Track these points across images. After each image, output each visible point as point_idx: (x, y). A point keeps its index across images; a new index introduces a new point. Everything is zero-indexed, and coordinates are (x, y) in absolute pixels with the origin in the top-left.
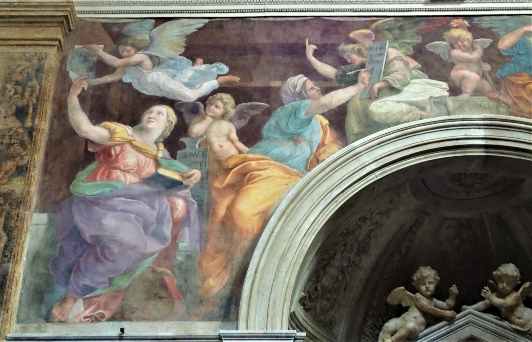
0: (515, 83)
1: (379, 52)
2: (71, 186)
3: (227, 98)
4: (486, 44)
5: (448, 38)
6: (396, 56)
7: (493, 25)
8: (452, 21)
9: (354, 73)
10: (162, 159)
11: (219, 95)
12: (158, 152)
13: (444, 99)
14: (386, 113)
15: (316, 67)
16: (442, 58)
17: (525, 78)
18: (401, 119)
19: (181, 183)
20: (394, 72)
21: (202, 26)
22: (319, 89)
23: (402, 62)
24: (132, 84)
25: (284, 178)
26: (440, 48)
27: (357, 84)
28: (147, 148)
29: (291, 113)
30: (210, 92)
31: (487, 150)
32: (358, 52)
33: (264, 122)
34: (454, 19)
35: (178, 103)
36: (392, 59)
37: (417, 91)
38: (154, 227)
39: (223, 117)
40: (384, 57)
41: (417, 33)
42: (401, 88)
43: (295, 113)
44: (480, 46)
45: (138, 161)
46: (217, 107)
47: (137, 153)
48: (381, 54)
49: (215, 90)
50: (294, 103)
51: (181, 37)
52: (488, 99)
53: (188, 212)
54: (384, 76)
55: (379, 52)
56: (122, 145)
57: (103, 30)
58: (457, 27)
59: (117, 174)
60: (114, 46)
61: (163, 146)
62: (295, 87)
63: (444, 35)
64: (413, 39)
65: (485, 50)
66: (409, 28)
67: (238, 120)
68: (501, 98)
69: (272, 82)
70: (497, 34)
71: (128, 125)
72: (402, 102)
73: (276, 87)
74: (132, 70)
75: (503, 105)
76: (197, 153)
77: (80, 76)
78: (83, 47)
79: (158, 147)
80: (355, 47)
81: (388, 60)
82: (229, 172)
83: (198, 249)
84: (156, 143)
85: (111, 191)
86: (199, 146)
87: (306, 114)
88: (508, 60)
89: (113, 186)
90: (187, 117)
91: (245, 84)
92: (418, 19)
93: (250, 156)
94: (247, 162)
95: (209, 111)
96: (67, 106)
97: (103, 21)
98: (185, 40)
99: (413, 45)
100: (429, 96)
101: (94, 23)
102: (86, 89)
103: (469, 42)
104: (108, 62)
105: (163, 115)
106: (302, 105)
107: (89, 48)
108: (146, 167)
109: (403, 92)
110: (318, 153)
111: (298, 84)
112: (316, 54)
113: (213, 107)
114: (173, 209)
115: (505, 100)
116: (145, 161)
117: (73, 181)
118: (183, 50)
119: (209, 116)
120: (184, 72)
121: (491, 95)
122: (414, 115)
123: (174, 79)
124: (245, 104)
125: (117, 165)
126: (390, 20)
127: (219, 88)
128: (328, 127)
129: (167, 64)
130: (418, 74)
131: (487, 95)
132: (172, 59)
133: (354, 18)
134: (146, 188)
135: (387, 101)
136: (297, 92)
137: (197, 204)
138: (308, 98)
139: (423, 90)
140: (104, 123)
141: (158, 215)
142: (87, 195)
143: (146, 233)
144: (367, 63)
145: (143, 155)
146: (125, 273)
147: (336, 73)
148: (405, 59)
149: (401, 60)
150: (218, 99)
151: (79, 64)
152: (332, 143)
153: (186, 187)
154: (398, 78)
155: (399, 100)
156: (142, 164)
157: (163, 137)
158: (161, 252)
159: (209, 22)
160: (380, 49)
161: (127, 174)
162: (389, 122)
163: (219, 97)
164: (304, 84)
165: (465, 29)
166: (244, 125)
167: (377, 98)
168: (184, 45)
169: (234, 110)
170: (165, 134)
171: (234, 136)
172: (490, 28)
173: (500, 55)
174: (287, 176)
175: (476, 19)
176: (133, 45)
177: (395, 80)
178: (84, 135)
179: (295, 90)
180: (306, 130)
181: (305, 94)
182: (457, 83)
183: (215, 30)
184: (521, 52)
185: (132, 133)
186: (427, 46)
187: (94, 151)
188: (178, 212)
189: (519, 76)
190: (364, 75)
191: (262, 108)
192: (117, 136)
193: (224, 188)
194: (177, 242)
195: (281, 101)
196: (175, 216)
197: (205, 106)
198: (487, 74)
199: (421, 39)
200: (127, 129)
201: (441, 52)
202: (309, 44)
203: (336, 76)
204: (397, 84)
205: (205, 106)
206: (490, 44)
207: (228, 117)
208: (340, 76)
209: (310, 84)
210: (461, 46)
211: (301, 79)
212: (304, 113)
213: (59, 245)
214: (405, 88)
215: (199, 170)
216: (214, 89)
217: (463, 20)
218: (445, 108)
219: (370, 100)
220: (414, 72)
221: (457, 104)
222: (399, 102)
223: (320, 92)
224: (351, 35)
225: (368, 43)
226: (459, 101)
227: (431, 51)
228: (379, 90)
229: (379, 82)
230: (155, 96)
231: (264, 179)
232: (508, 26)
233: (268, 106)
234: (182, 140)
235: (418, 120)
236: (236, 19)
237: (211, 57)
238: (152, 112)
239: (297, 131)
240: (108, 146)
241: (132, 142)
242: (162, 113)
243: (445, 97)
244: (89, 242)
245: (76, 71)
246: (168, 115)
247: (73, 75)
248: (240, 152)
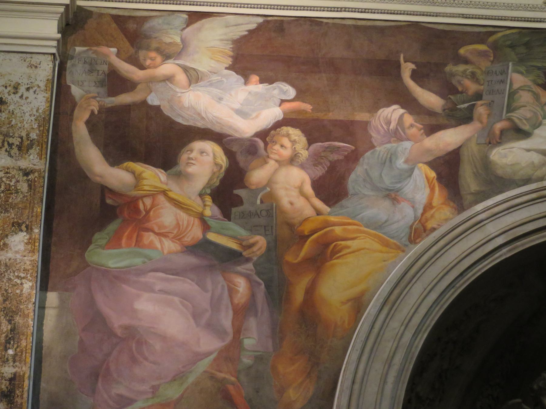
1: (500, 77)
2: (86, 254)
3: (295, 133)
6: (522, 84)
9: (468, 107)
10: (210, 219)
11: (286, 129)
12: (204, 209)
15: (416, 96)
19: (240, 254)
20: (521, 107)
21: (254, 28)
22: (421, 126)
23: (530, 94)
24: (162, 108)
25: (381, 252)
27: (472, 123)
28: (188, 202)
29: (386, 160)
30: (271, 125)
32: (471, 76)
33: (349, 171)
35: (228, 138)
38: (208, 315)
39: (292, 160)
40: (506, 86)
43: (391, 158)
45: (177, 220)
46: (282, 146)
47: (174, 209)
49: (278, 121)
50: (388, 146)
51: (226, 42)
53: (253, 296)
54: (508, 112)
55: (500, 77)
56: (153, 196)
57: (114, 25)
59: (149, 238)
60: (132, 50)
61: (211, 200)
62: (389, 123)
67: (313, 167)
69: (356, 113)
71: (159, 168)
73: (362, 121)
74: (160, 86)
76: (259, 212)
77: (86, 92)
78: (88, 50)
79: (204, 201)
80: (468, 69)
82: (306, 241)
83: (271, 349)
84: (201, 195)
85: (144, 263)
86: (262, 202)
87: (406, 162)
89: (146, 256)
90: (241, 159)
91: (320, 115)
93: (333, 219)
94: (329, 227)
95: (272, 152)
96: (72, 137)
97: (114, 12)
98: (232, 46)
101: (101, 15)
102: (96, 112)
104: (125, 74)
105: (208, 155)
106: (400, 149)
107: (95, 52)
108: (190, 230)
110: (424, 218)
111: (393, 118)
112: (414, 76)
113: (277, 147)
114: (232, 291)
116: (188, 221)
117: (88, 247)
118: (229, 61)
119: (271, 158)
120: (233, 93)
123: (220, 103)
124: (320, 144)
125: (148, 225)
126: (513, 33)
127: (284, 119)
128: (435, 181)
129: (209, 81)
132: (215, 73)
133: (465, 27)
134: (192, 260)
135: (513, 148)
136: (391, 130)
137: (265, 286)
138: (408, 139)
140: (125, 164)
141: (212, 298)
142: (110, 268)
143: (198, 325)
144: (484, 93)
145: (183, 212)
146: (174, 379)
147: (443, 106)
148: (534, 90)
149: (529, 90)
150: (283, 136)
151: (84, 75)
152: (443, 204)
153: (248, 260)
155: (528, 147)
156: (183, 225)
157: (210, 187)
158: (221, 352)
159: (264, 21)
160: (501, 74)
161: (163, 239)
162: (516, 178)
163: (285, 132)
164: (401, 117)
166: (321, 174)
167: (499, 143)
168: (231, 54)
169: (307, 151)
170: (212, 182)
171: (308, 189)
174: (384, 249)
176: (158, 50)
178: (98, 179)
179: (390, 126)
180: (407, 185)
181: (403, 134)
183: (273, 35)
185: (166, 179)
187: (116, 204)
188: (239, 295)
190: (481, 110)
191: (346, 151)
192: (145, 184)
193: (299, 264)
194: (241, 337)
195: (371, 142)
196: (236, 301)
197: (266, 144)
200: (160, 174)
202: (405, 62)
203: (444, 110)
204: (525, 125)
205: (266, 144)
207: (298, 162)
208: (448, 109)
209: (409, 119)
211: (396, 111)
212: (403, 160)
213: (78, 338)
214: (536, 131)
215: (263, 237)
216: (276, 120)
219: (490, 145)
222: (528, 150)
223: (422, 131)
224: (462, 51)
225: (485, 64)
228: (502, 131)
229: (501, 120)
230: (195, 127)
231: (353, 252)
233: (353, 148)
234: (236, 192)
236: (303, 19)
237: (271, 74)
238: (192, 151)
239: (395, 185)
240: (134, 197)
241: (166, 192)
242: (206, 153)
244: (119, 334)
245: (80, 84)
246: (214, 155)
247: (76, 91)
248: (319, 213)
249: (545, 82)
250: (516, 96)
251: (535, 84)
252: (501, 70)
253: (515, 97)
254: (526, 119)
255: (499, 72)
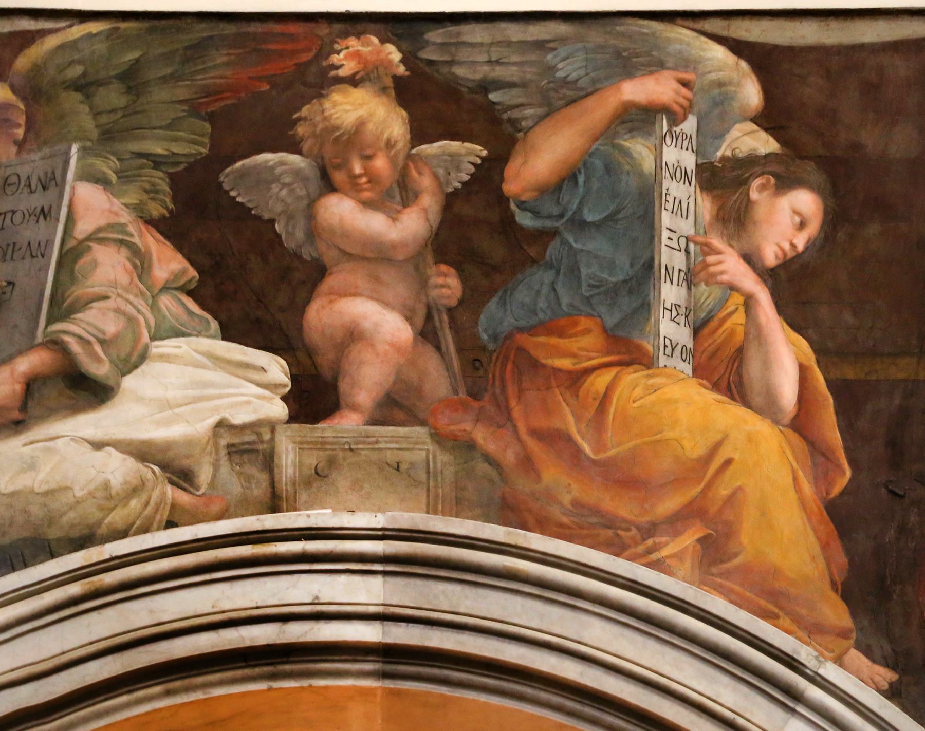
0: (544, 366)
1: (38, 200)
4: (458, 169)
5: (314, 135)
6: (102, 222)
7: (499, 72)
8: (337, 47)
13: (267, 436)
14: (47, 493)
16: (279, 236)
17: (586, 341)
18: (99, 523)
20: (92, 301)
23: (125, 252)
26: (275, 188)
31: (390, 668)
34: (346, 35)
36: (89, 238)
37: (171, 394)
41: (194, 108)
42: (111, 382)
44: (436, 176)
48: (45, 214)
52: (428, 440)
54: (50, 321)
55: (38, 200)
58: (353, 81)
63: (299, 119)
64: (176, 139)
65: (450, 201)
66: (164, 80)
68: (481, 435)
70: (510, 120)
72: (108, 444)
75: (483, 467)
81: (71, 244)
88: (533, 252)
92: (202, 30)
99: (172, 170)
100: (212, 420)
103: (393, 160)
109: (117, 400)
115: (491, 447)
121: (444, 421)
122: (147, 504)
126: (90, 36)
130: (180, 311)
131: (431, 420)
135: (58, 437)
139: (197, 392)
148: (136, 240)
149: (122, 242)
154: (104, 333)
162: (53, 534)
165: (384, 90)
172: (485, 86)
173: (508, 224)
175: (435, 36)
177: (92, 339)
182: (325, 361)
184: (590, 216)
186: (227, 177)
189: (561, 334)
198: (445, 318)
199: (206, 140)
201: (279, 208)
204: (99, 360)
206: (472, 169)
210: (360, 176)
214: (129, 382)
217: (383, 41)
218: (263, 477)
220: (166, 302)
221: (312, 459)
222: (98, 446)
226: (321, 445)
227: (239, 199)
232: (560, 74)
235: (158, 529)
243: (272, 425)
249: (171, 212)
250: (82, 263)
251: (141, 217)
252: (46, 173)
253: (77, 267)
254: (102, 342)
255: (40, 180)
